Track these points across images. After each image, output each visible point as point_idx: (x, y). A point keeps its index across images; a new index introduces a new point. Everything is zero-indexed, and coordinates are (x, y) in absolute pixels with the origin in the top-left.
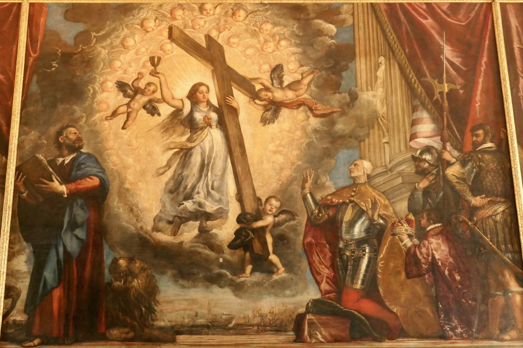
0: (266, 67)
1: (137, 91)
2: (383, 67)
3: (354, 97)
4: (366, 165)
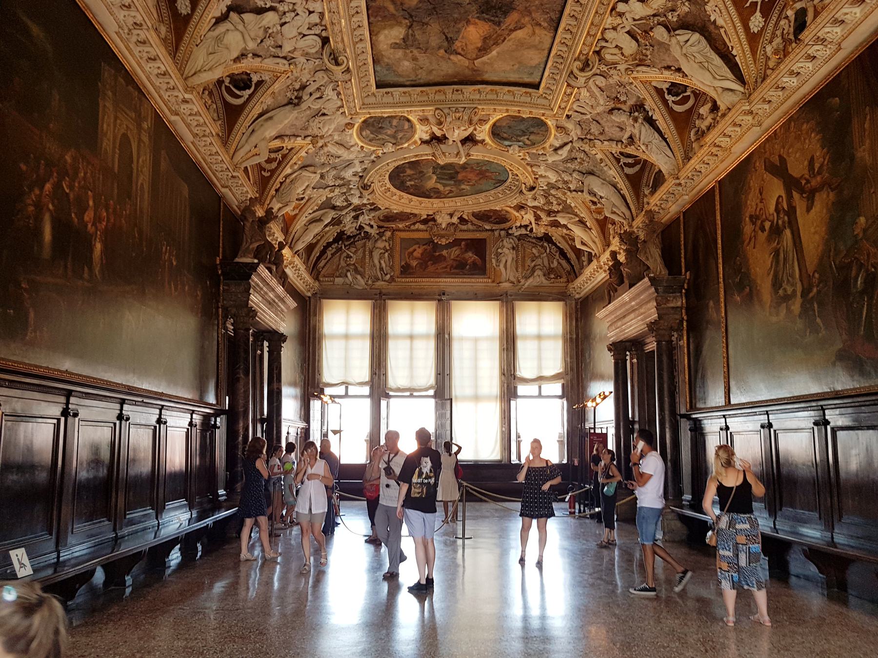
0: (806, 163)
1: (757, 218)
2: (868, 117)
3: (852, 158)
4: (862, 220)
